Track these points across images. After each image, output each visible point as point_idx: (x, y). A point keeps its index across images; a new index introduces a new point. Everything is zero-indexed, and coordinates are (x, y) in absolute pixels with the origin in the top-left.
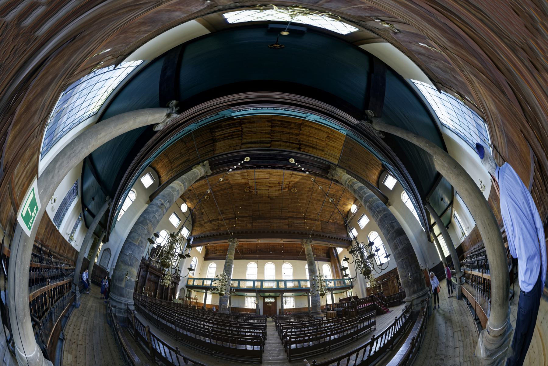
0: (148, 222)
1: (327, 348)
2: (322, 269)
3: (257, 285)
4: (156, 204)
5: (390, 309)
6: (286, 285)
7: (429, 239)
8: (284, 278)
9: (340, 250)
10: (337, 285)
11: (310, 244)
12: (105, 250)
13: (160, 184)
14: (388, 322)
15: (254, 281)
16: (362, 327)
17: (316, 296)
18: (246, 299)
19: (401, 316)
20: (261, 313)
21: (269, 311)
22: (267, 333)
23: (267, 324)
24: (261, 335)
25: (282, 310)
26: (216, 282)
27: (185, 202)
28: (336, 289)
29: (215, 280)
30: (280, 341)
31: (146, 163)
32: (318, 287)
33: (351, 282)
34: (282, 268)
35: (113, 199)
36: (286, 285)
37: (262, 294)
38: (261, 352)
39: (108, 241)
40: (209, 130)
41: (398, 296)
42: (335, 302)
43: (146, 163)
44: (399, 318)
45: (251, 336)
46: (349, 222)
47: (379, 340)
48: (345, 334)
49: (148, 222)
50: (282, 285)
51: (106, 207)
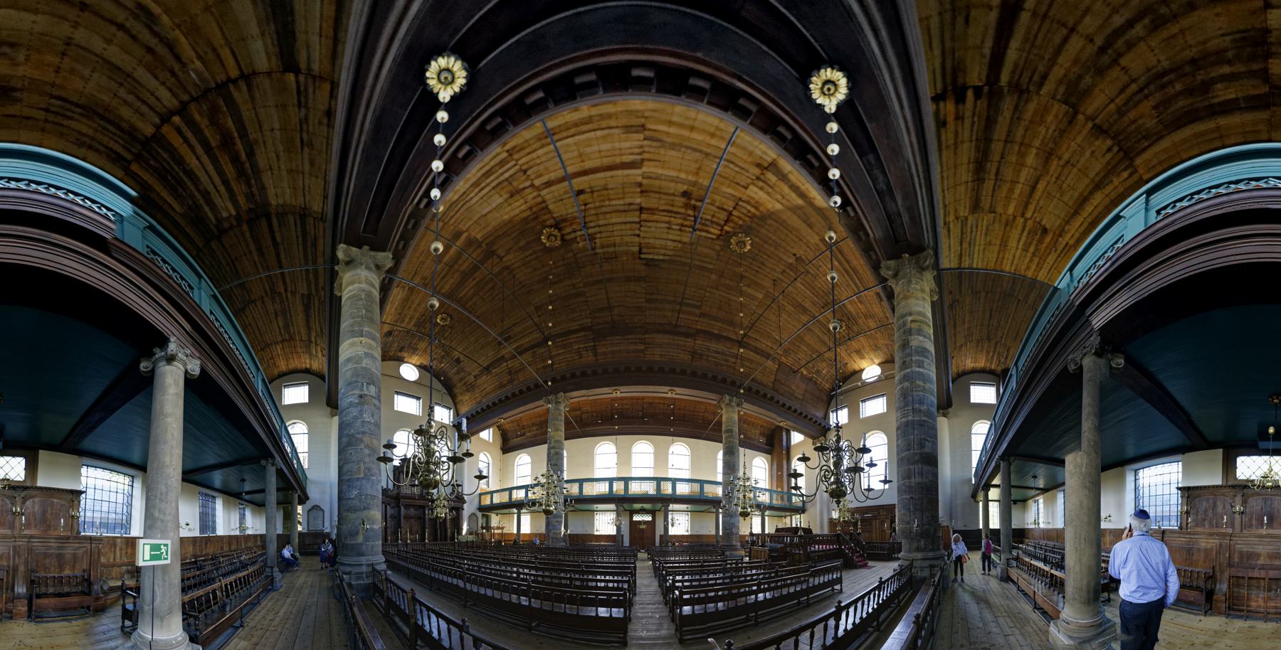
3: (618, 488)
5: (870, 563)
7: (974, 496)
8: (672, 474)
15: (611, 481)
18: (597, 517)
20: (627, 543)
21: (642, 539)
22: (638, 582)
23: (638, 564)
24: (626, 586)
25: (666, 537)
26: (536, 489)
29: (533, 486)
37: (627, 506)
38: (626, 620)
45: (606, 588)
46: (842, 394)
50: (667, 489)
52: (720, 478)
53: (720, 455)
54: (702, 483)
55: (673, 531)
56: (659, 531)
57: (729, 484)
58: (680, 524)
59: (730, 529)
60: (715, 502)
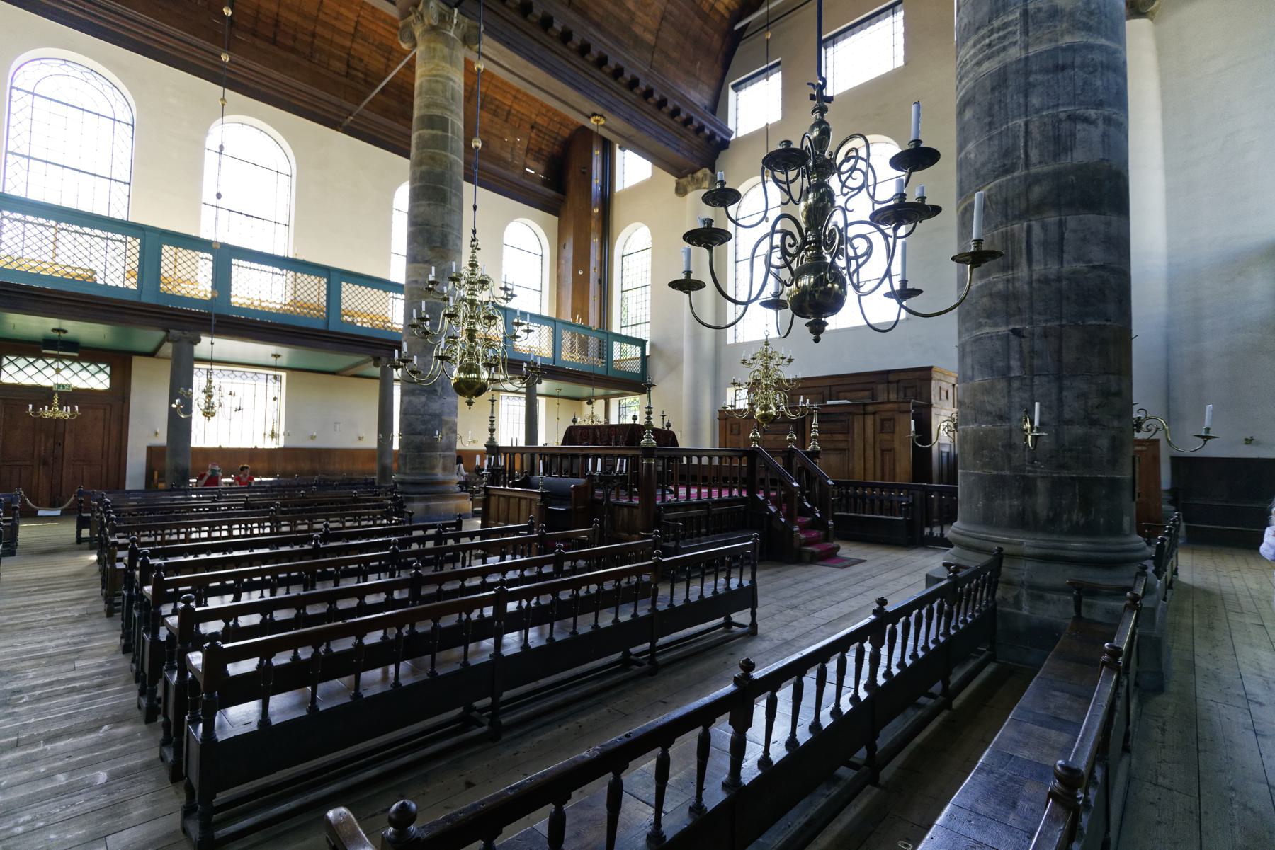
1: (480, 708)
2: (499, 244)
6: (222, 279)
9: (632, 168)
10: (566, 355)
11: (462, 53)
14: (833, 612)
16: (679, 600)
17: (431, 391)
19: (919, 603)
25: (177, 460)
28: (553, 371)
30: (133, 696)
32: (453, 339)
33: (644, 358)
34: (199, 147)
36: (222, 279)
41: (904, 499)
42: (541, 443)
44: (905, 610)
46: (768, 23)
47: (785, 695)
48: (585, 625)
50: (191, 278)
52: (398, 271)
53: (402, 196)
54: (335, 277)
55: (204, 435)
56: (147, 427)
57: (425, 294)
58: (244, 409)
59: (426, 431)
60: (378, 346)
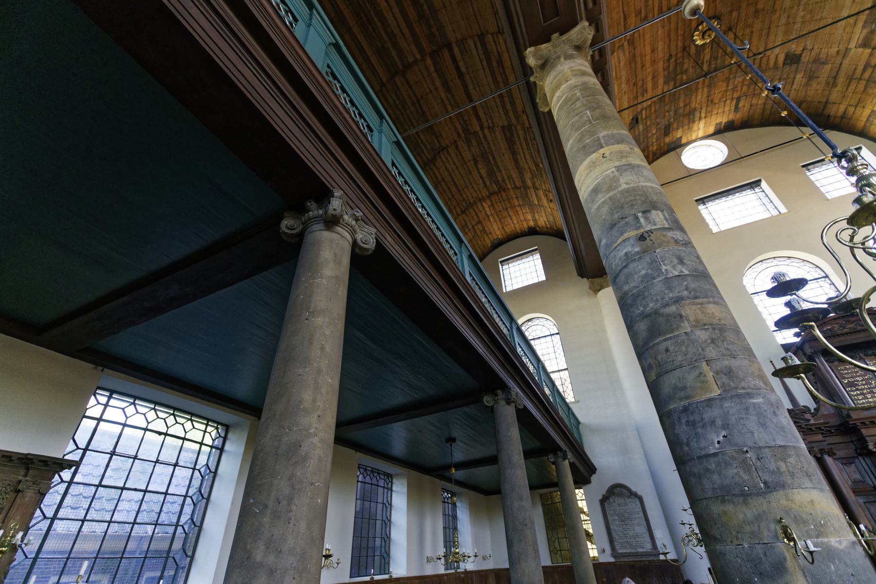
0: (673, 309)
4: (629, 258)
12: (604, 501)
13: (559, 234)
27: (677, 146)
31: (467, 268)
35: (505, 387)
39: (592, 470)
40: (398, 80)
43: (467, 268)
49: (673, 309)
51: (507, 414)
